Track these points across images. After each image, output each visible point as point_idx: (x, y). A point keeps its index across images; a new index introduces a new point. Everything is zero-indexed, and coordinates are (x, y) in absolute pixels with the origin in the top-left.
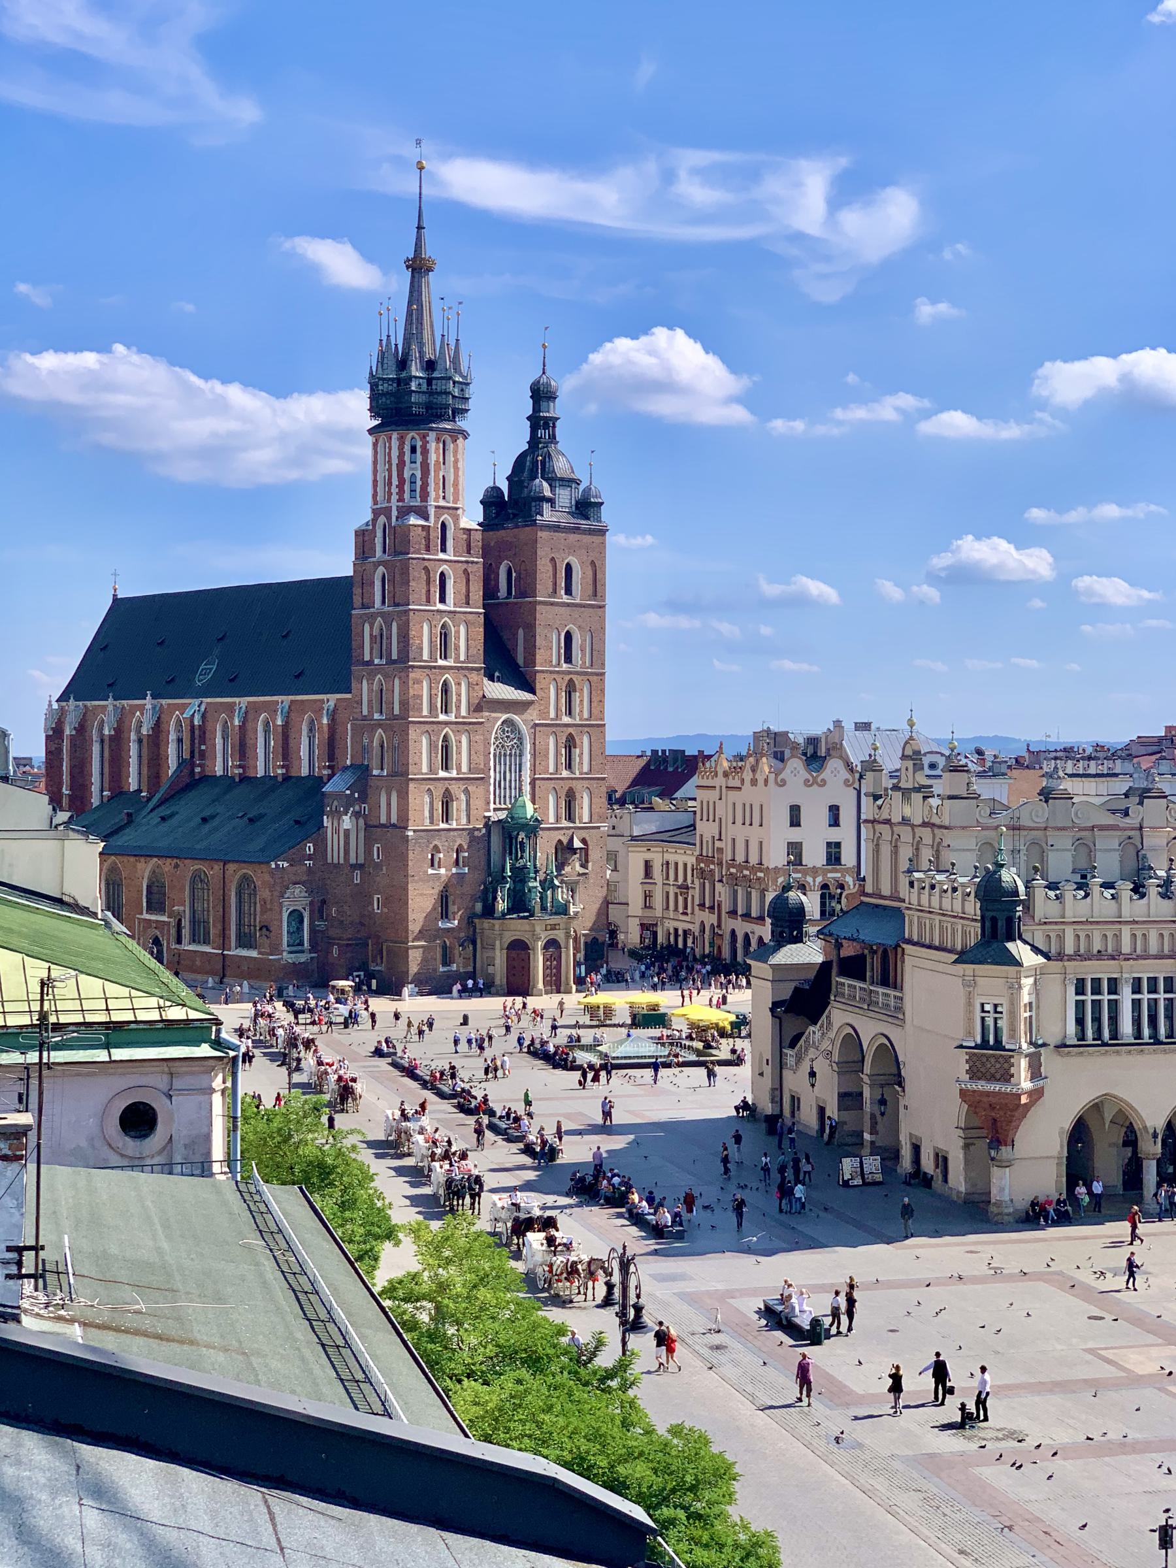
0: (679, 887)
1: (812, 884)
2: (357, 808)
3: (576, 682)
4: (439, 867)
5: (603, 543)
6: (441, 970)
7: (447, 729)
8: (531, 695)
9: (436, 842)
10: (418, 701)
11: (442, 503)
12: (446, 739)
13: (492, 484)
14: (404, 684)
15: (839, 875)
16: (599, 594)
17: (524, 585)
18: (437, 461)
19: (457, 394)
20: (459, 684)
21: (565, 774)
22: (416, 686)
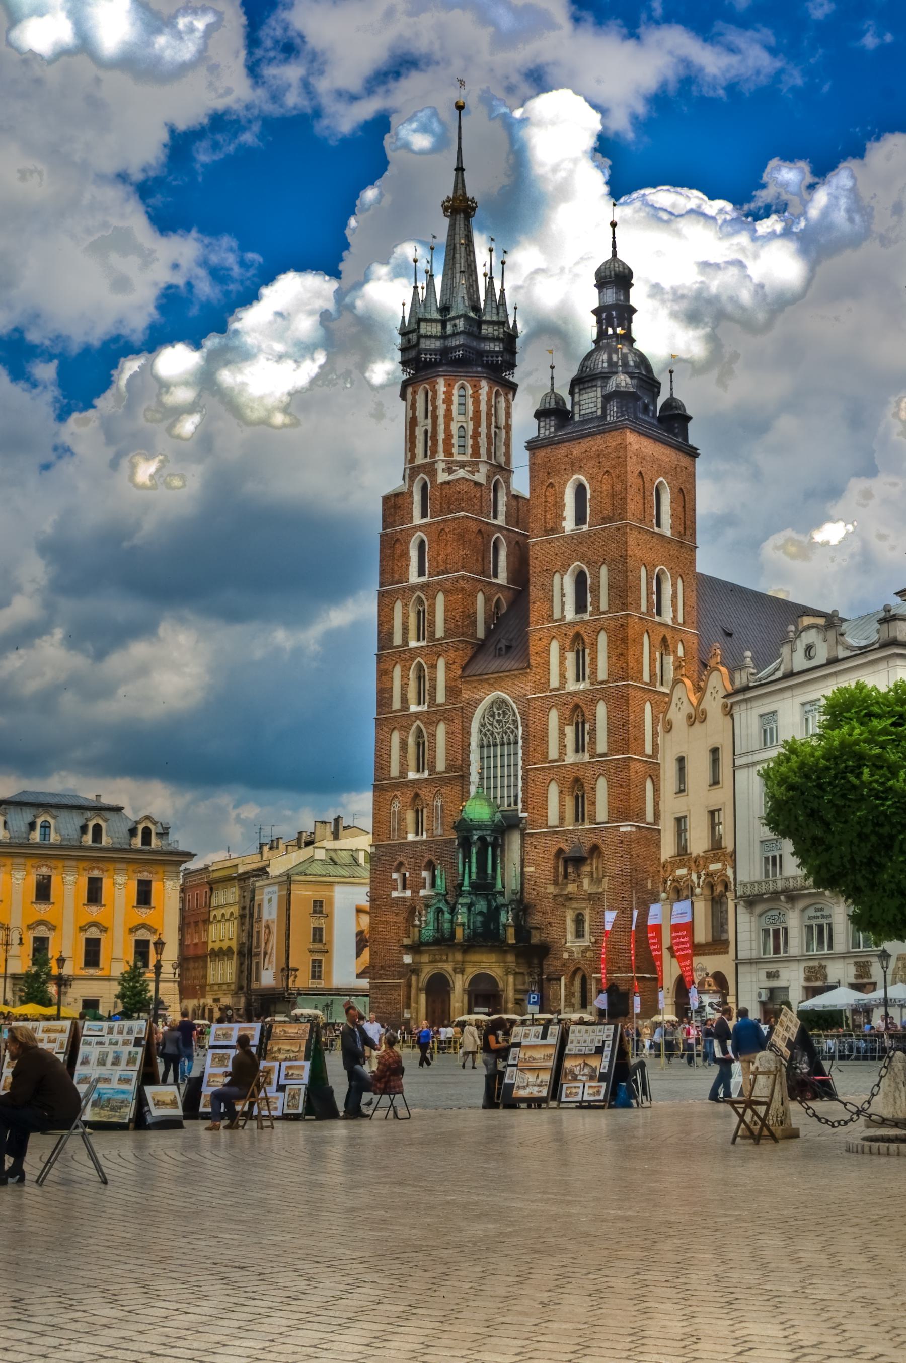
7: (418, 722)
9: (401, 859)
10: (387, 695)
11: (420, 460)
20: (434, 667)
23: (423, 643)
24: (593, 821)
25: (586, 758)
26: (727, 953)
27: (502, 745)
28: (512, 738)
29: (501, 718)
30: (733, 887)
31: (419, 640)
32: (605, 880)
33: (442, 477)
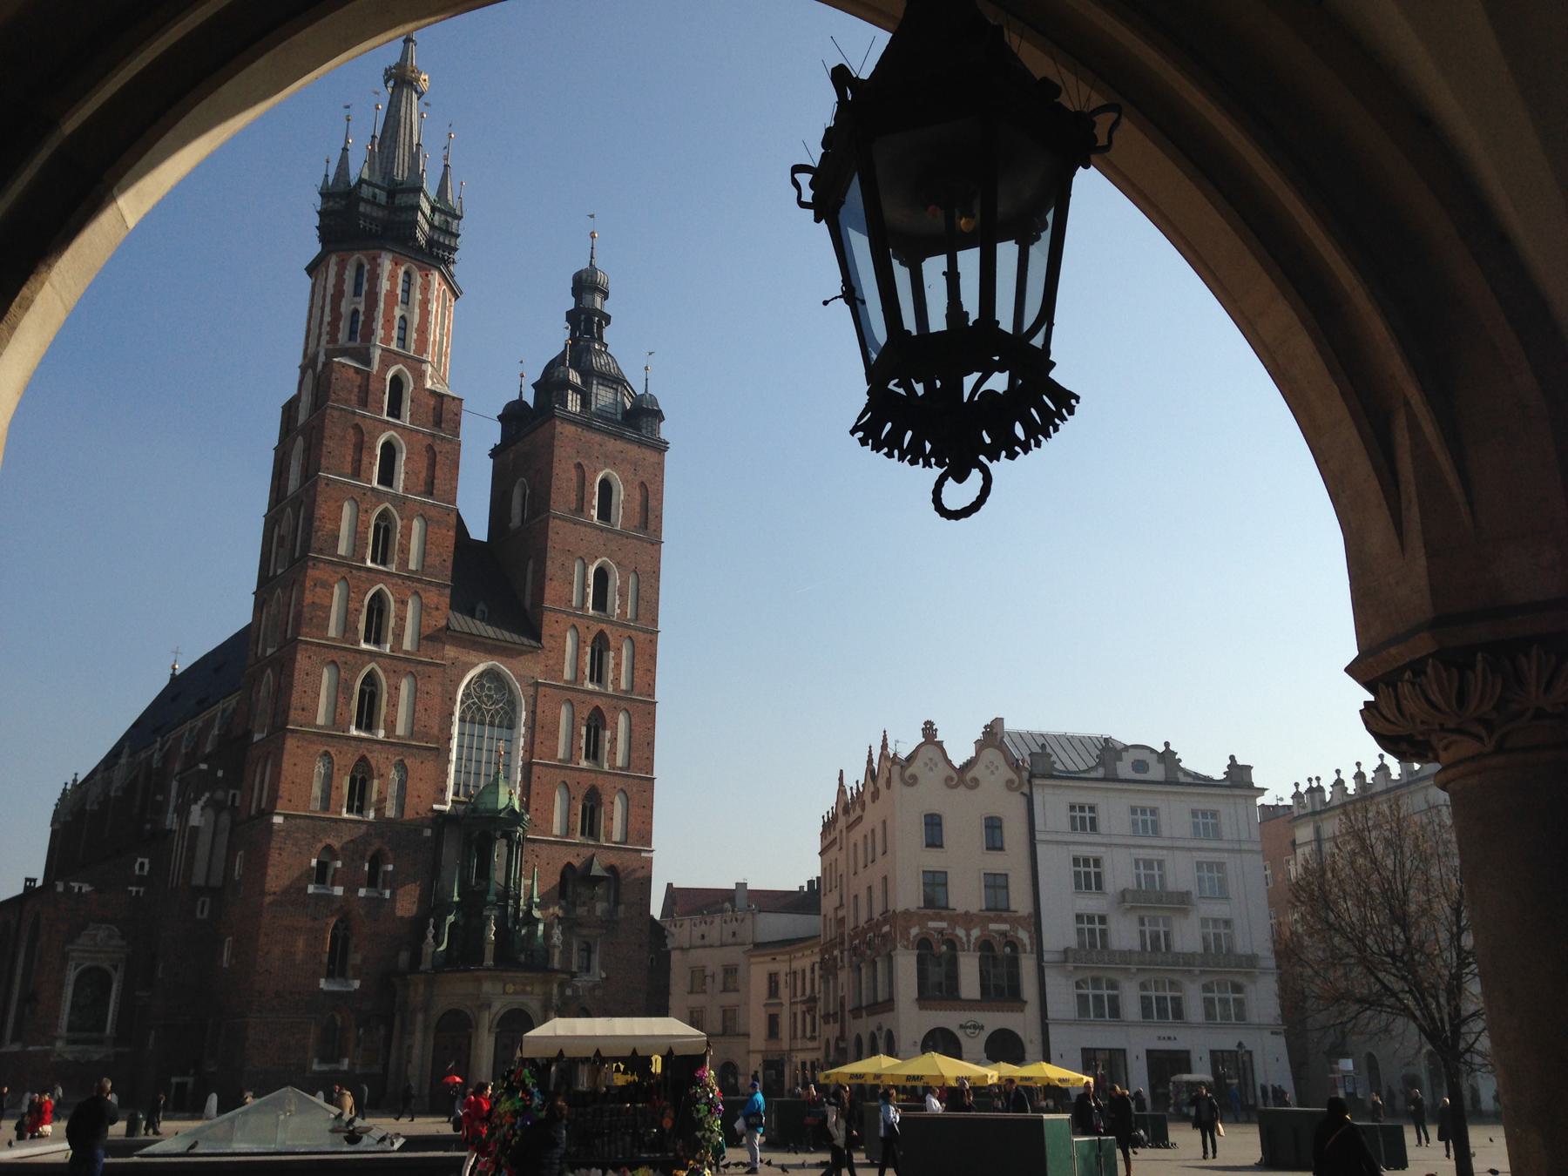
0: (803, 1002)
1: (965, 939)
2: (220, 795)
3: (610, 638)
4: (333, 884)
5: (660, 466)
6: (315, 1067)
7: (373, 665)
8: (534, 643)
9: (328, 841)
10: (320, 613)
11: (393, 346)
12: (371, 679)
13: (518, 398)
14: (303, 585)
15: (1004, 927)
16: (651, 527)
17: (539, 504)
18: (391, 293)
19: (436, 223)
20: (404, 603)
21: (584, 764)
22: (318, 589)
23: (381, 568)
24: (609, 837)
25: (606, 766)
26: (1022, 1011)
27: (492, 724)
28: (505, 723)
29: (493, 692)
30: (1028, 948)
31: (374, 560)
32: (622, 908)
33: (429, 385)
